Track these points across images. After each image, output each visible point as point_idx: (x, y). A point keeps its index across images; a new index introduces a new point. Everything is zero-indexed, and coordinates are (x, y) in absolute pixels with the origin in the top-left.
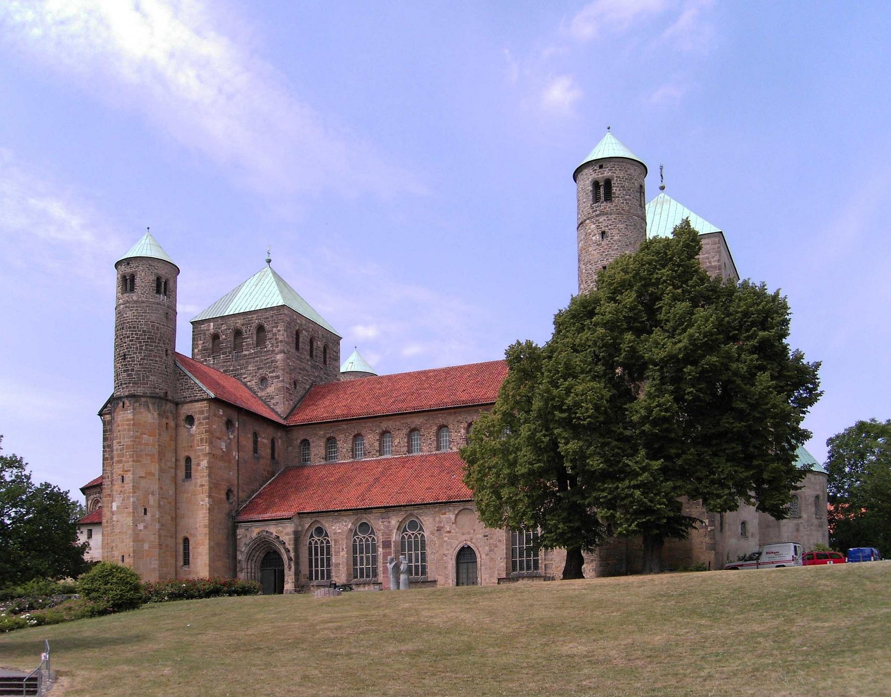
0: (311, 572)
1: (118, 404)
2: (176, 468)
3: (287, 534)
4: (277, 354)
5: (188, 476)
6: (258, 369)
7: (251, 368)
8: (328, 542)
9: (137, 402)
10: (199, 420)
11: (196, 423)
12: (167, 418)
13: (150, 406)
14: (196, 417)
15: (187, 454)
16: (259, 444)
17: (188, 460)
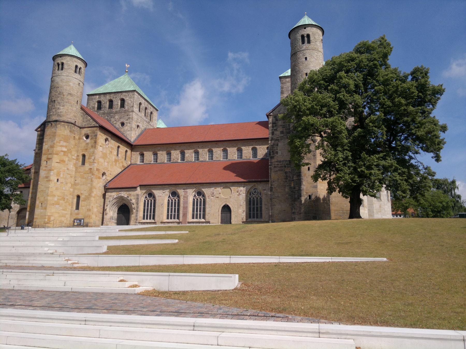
0: (144, 215)
1: (48, 124)
2: (77, 159)
3: (134, 196)
4: (130, 112)
5: (83, 163)
6: (120, 118)
7: (117, 117)
8: (155, 201)
9: (59, 124)
10: (92, 136)
11: (90, 138)
12: (75, 134)
13: (66, 127)
14: (90, 135)
15: (84, 153)
16: (119, 152)
17: (84, 156)
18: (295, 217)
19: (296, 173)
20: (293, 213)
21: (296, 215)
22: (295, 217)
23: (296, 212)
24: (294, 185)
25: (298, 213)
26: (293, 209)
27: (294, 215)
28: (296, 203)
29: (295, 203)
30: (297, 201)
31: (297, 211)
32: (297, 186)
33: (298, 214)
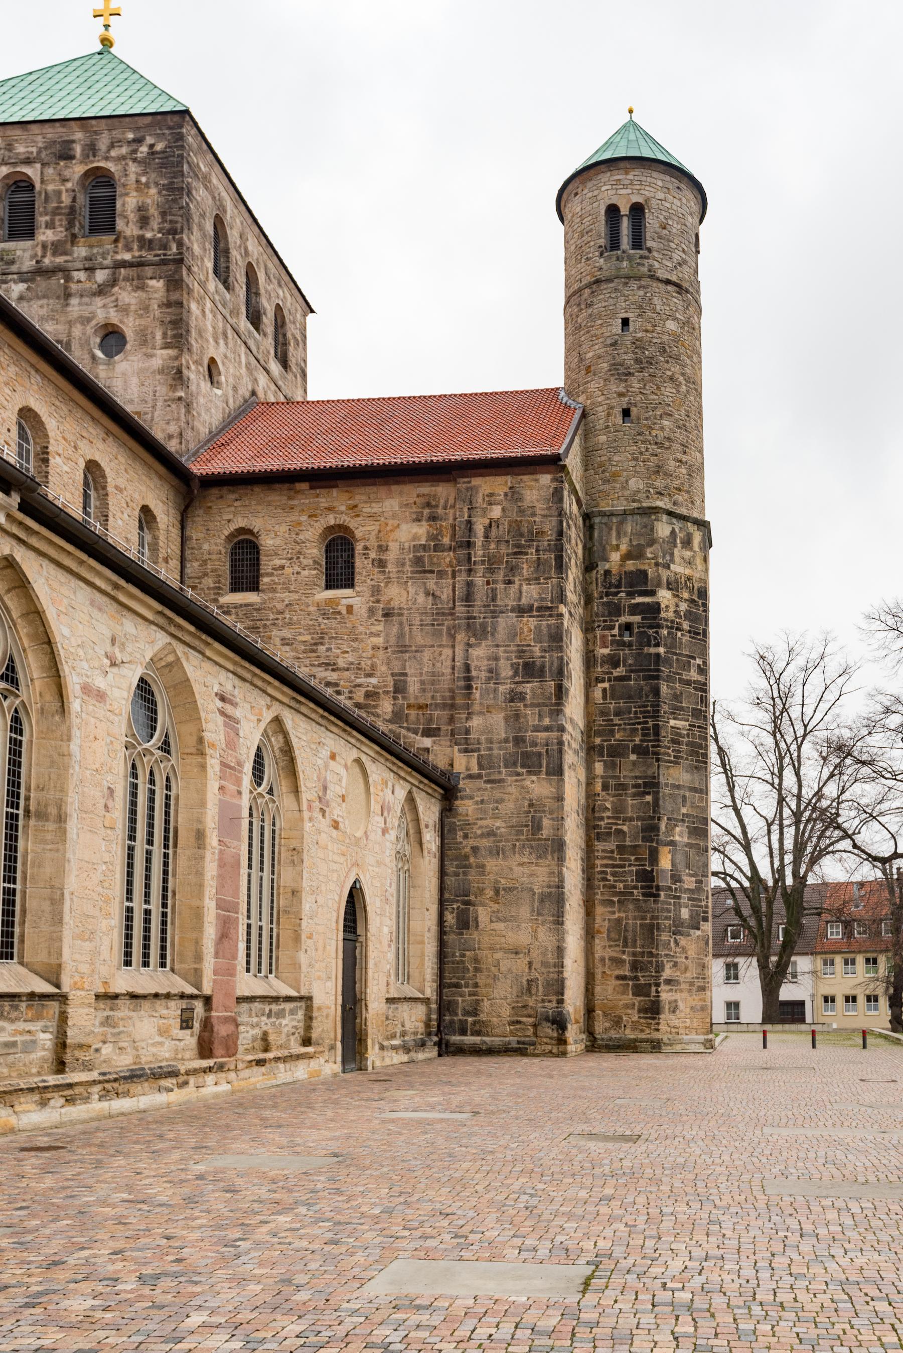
18: (676, 1001)
19: (687, 815)
20: (668, 982)
21: (681, 991)
22: (676, 1001)
23: (682, 980)
24: (673, 864)
25: (692, 984)
26: (668, 966)
27: (671, 990)
28: (683, 941)
29: (677, 943)
30: (689, 935)
31: (688, 975)
32: (692, 876)
33: (690, 991)
